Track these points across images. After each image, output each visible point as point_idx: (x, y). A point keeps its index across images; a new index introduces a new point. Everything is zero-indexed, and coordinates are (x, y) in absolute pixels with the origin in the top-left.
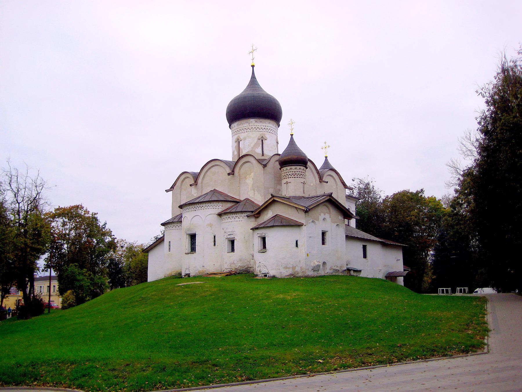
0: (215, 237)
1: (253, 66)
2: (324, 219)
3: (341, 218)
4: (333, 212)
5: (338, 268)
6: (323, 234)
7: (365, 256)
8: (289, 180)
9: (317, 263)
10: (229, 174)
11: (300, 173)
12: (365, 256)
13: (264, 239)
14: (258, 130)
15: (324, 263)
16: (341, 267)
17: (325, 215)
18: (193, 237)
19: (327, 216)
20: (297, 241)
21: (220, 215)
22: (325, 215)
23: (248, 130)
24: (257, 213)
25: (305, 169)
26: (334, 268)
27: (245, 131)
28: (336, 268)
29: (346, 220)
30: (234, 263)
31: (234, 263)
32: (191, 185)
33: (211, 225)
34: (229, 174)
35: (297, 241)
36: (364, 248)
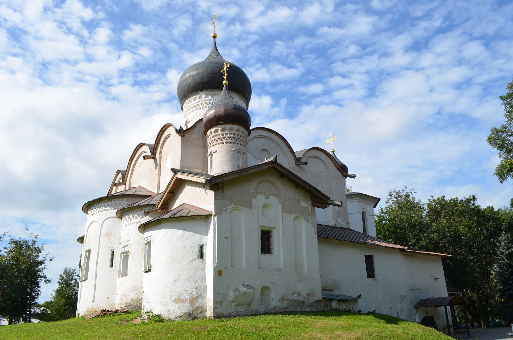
0: (113, 252)
1: (215, 37)
2: (265, 206)
3: (305, 204)
4: (289, 192)
5: (301, 298)
9: (243, 289)
11: (232, 136)
12: (371, 273)
15: (265, 289)
16: (308, 295)
17: (267, 198)
19: (273, 201)
22: (267, 198)
23: (198, 107)
25: (246, 132)
26: (290, 297)
27: (194, 109)
28: (295, 297)
30: (125, 295)
31: (125, 295)
33: (108, 235)
35: (201, 247)
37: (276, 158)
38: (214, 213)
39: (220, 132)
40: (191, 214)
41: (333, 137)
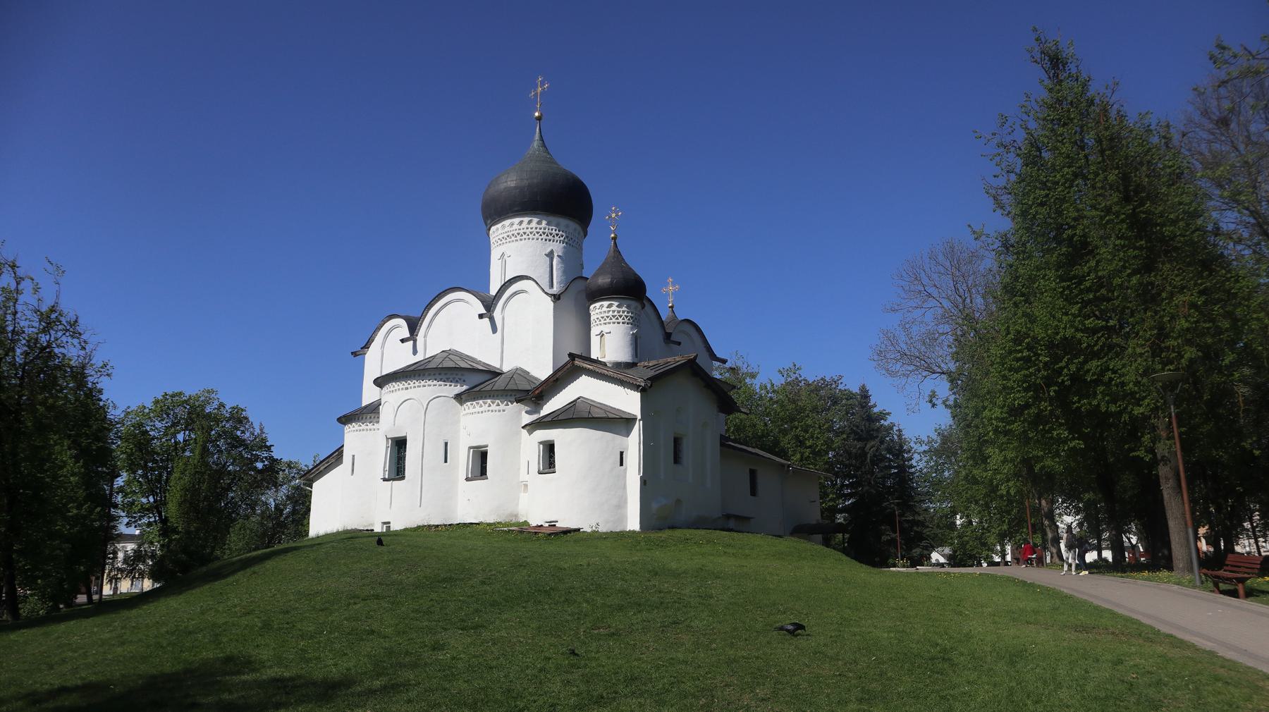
6: (677, 442)
7: (753, 492)
8: (606, 329)
10: (481, 316)
12: (753, 492)
13: (549, 448)
14: (544, 237)
18: (399, 445)
20: (622, 453)
21: (459, 398)
24: (534, 394)
29: (722, 416)
32: (403, 341)
34: (481, 316)
35: (622, 453)
36: (753, 474)
37: (696, 357)
38: (639, 417)
39: (614, 308)
40: (611, 416)
41: (674, 285)
